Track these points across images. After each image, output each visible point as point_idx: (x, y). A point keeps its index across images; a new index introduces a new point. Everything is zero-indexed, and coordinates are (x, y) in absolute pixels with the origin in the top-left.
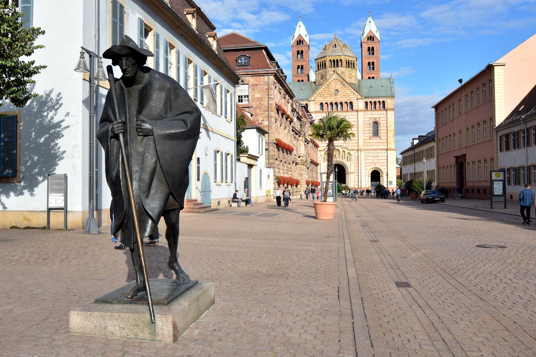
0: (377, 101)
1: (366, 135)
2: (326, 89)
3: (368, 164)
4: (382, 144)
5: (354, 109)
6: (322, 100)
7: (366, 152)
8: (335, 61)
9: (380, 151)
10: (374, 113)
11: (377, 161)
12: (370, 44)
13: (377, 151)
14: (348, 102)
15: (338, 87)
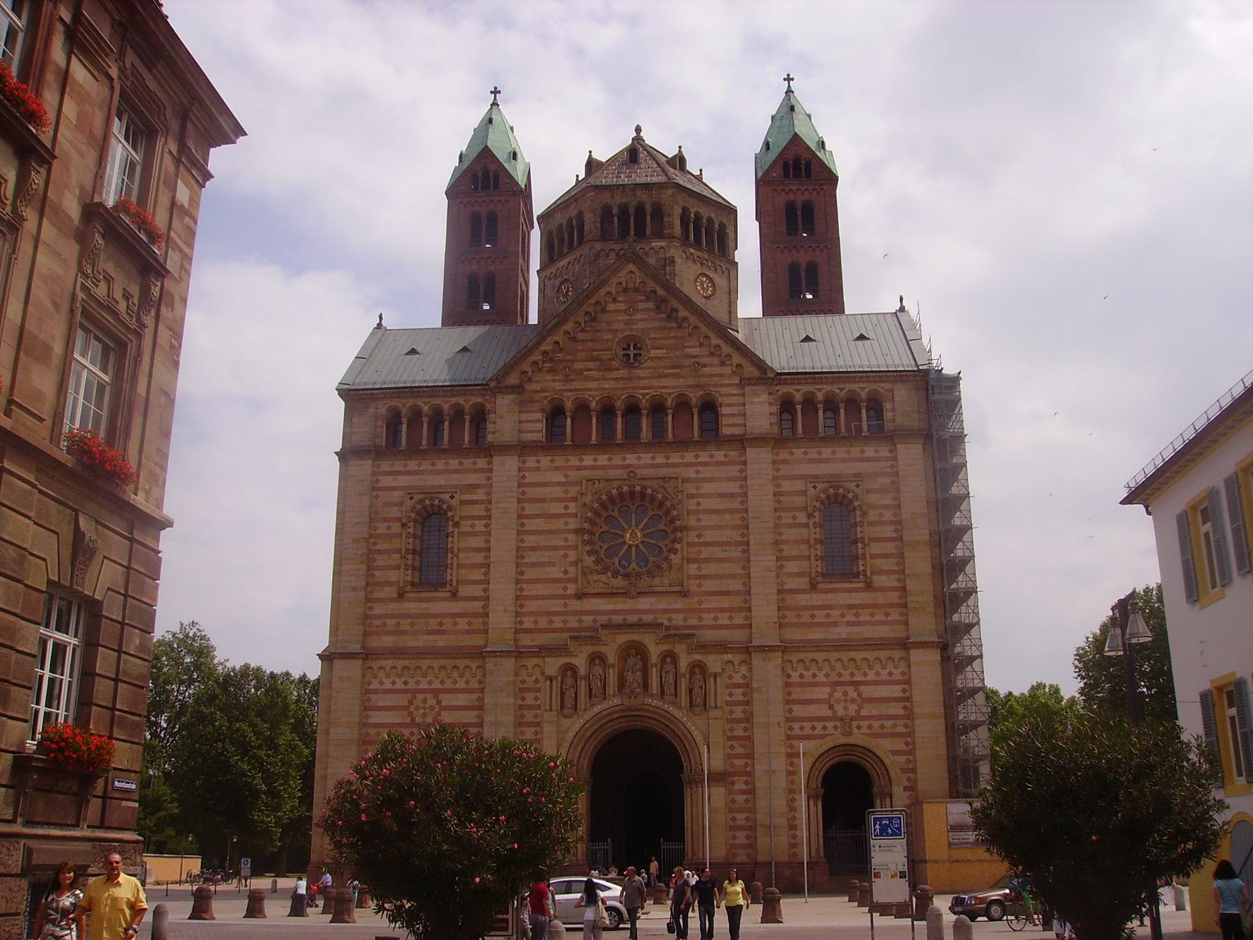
0: (842, 394)
1: (792, 567)
2: (580, 336)
3: (807, 725)
4: (880, 617)
5: (726, 431)
6: (558, 386)
7: (794, 657)
8: (632, 210)
9: (870, 655)
10: (827, 452)
11: (853, 708)
12: (794, 188)
13: (852, 654)
14: (694, 397)
15: (641, 325)
